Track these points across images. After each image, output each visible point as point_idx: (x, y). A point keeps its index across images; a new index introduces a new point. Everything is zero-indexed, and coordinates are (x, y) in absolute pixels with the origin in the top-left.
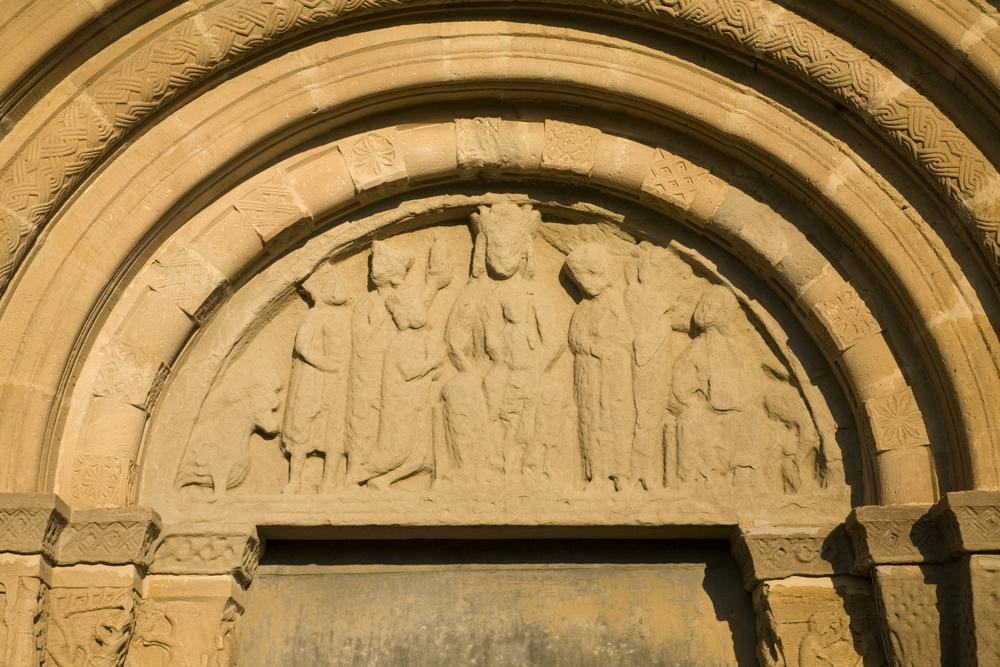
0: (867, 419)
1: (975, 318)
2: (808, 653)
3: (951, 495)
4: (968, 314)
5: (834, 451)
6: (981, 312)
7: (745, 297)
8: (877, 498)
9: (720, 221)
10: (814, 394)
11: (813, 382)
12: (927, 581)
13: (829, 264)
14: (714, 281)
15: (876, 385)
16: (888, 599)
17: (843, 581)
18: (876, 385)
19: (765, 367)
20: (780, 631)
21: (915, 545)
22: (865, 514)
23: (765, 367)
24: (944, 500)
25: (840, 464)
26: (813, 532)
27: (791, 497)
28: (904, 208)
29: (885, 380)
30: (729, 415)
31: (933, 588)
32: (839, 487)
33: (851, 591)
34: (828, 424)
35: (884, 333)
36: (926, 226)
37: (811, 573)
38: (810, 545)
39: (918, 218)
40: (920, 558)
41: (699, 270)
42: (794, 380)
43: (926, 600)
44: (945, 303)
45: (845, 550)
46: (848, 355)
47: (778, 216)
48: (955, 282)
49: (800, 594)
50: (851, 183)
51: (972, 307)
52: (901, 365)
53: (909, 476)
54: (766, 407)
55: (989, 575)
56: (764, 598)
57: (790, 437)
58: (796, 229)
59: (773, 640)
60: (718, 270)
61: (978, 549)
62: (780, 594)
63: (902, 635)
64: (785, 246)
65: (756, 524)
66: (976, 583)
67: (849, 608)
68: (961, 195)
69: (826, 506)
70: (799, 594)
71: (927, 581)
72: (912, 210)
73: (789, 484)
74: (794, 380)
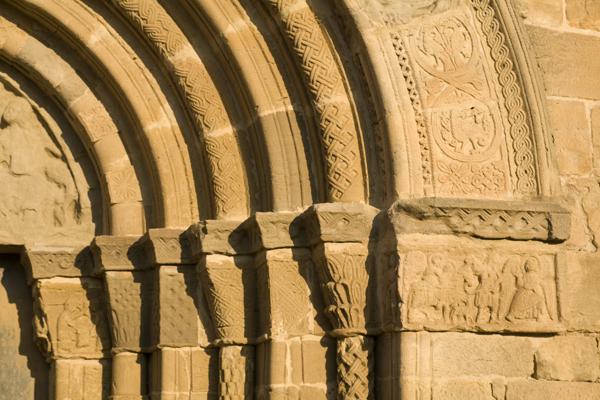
0: (106, 184)
1: (172, 128)
2: (63, 323)
3: (151, 230)
4: (168, 125)
5: (86, 202)
6: (176, 124)
7: (36, 105)
8: (110, 232)
9: (22, 57)
10: (77, 167)
11: (76, 160)
12: (135, 281)
13: (88, 89)
14: (18, 94)
15: (112, 164)
16: (111, 291)
17: (88, 280)
18: (112, 164)
19: (47, 150)
20: (46, 310)
21: (130, 259)
22: (101, 241)
23: (47, 150)
24: (147, 235)
25: (90, 211)
26: (70, 250)
27: (58, 229)
28: (135, 59)
29: (118, 161)
30: (22, 178)
31: (139, 285)
32: (88, 224)
33: (91, 287)
34: (84, 186)
35: (119, 133)
36: (147, 71)
37: (67, 275)
38: (68, 258)
39: (142, 65)
40: (132, 267)
41: (8, 87)
42: (64, 158)
43: (134, 292)
44: (155, 117)
45: (88, 262)
46: (97, 145)
47: (59, 58)
48: (161, 105)
49: (59, 288)
50: (103, 41)
51: (170, 120)
52: (128, 152)
53: (129, 220)
54: (46, 174)
55: (171, 278)
56: (38, 289)
57: (60, 193)
58: (69, 66)
59: (42, 315)
60: (21, 88)
61: (164, 262)
62: (48, 288)
63: (118, 312)
64: (62, 76)
65: (34, 246)
66: (162, 282)
67: (89, 296)
68: (167, 54)
69: (80, 234)
70: (60, 289)
71: (135, 281)
72: (139, 61)
73: (58, 221)
74: (64, 158)
